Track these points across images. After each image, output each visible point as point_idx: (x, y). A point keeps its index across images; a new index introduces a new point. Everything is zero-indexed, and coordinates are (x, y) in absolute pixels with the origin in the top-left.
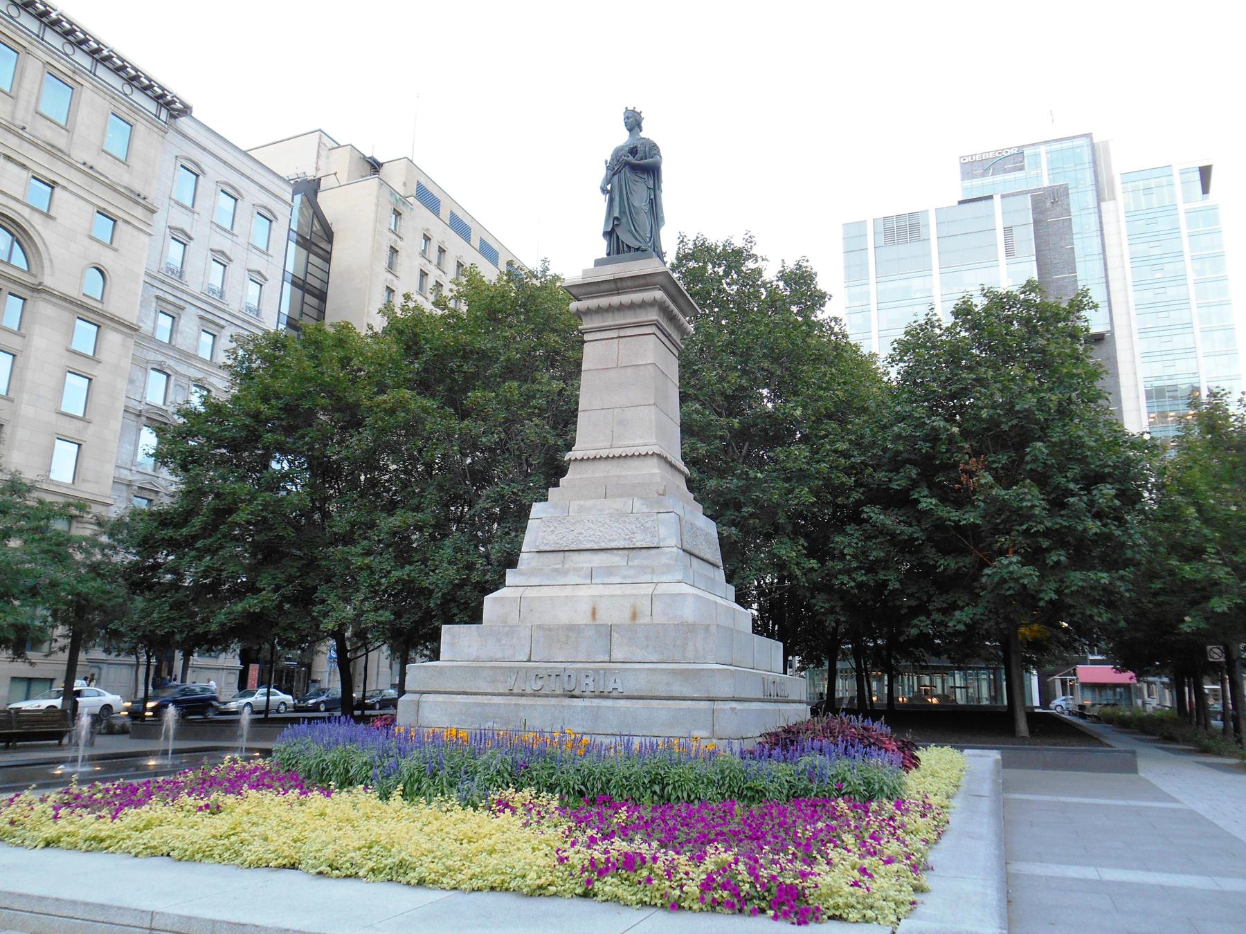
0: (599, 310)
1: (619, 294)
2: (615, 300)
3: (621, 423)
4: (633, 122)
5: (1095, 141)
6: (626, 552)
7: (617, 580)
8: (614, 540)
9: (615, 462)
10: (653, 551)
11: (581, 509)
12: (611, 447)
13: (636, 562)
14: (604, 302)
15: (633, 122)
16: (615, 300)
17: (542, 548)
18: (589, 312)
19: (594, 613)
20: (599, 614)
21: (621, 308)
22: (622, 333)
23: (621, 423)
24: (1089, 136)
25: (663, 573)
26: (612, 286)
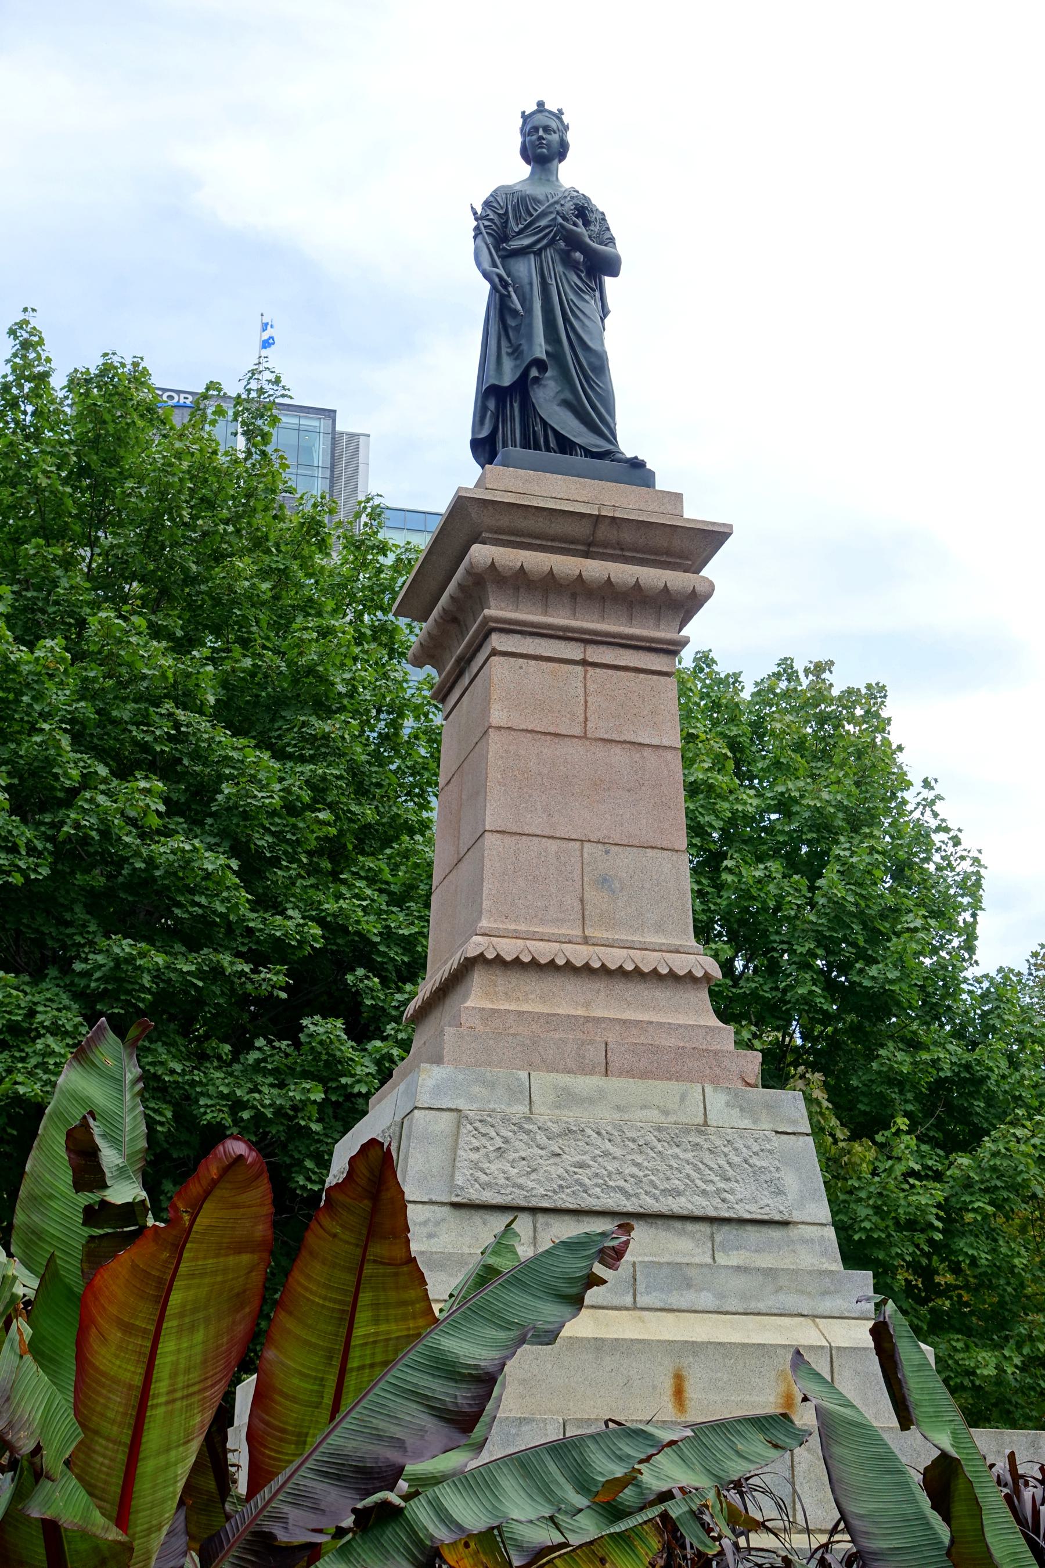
0: (548, 588)
1: (587, 555)
2: (595, 569)
3: (604, 882)
4: (544, 142)
5: (338, 428)
6: (705, 1228)
7: (706, 1300)
8: (676, 1193)
9: (600, 985)
10: (776, 1233)
11: (566, 1098)
12: (586, 941)
13: (735, 1259)
14: (566, 565)
15: (544, 142)
16: (595, 569)
17: (475, 1194)
18: (520, 583)
19: (679, 1393)
20: (693, 1392)
21: (580, 592)
22: (596, 654)
23: (604, 882)
24: (330, 414)
25: (825, 1293)
26: (581, 530)
